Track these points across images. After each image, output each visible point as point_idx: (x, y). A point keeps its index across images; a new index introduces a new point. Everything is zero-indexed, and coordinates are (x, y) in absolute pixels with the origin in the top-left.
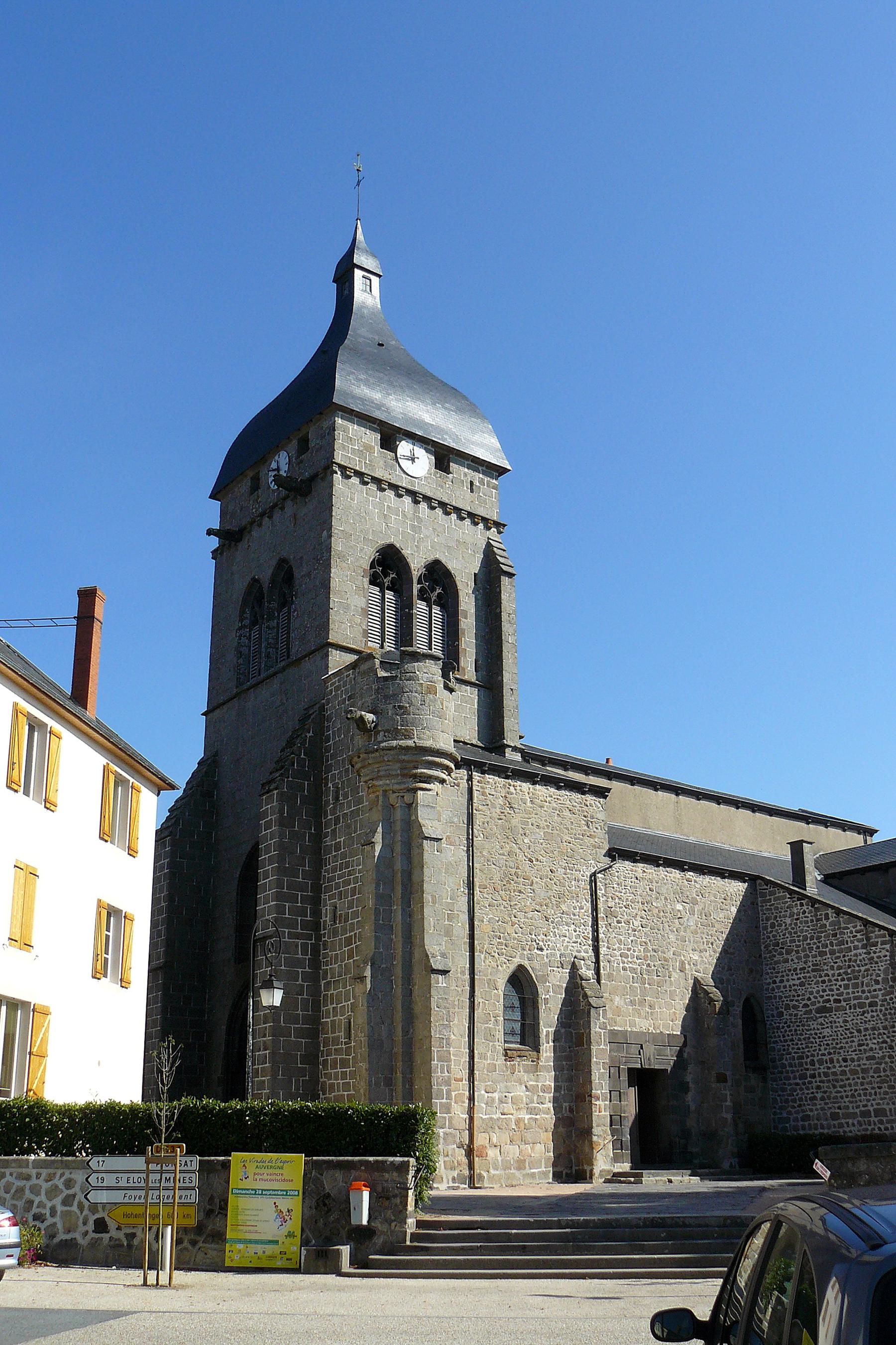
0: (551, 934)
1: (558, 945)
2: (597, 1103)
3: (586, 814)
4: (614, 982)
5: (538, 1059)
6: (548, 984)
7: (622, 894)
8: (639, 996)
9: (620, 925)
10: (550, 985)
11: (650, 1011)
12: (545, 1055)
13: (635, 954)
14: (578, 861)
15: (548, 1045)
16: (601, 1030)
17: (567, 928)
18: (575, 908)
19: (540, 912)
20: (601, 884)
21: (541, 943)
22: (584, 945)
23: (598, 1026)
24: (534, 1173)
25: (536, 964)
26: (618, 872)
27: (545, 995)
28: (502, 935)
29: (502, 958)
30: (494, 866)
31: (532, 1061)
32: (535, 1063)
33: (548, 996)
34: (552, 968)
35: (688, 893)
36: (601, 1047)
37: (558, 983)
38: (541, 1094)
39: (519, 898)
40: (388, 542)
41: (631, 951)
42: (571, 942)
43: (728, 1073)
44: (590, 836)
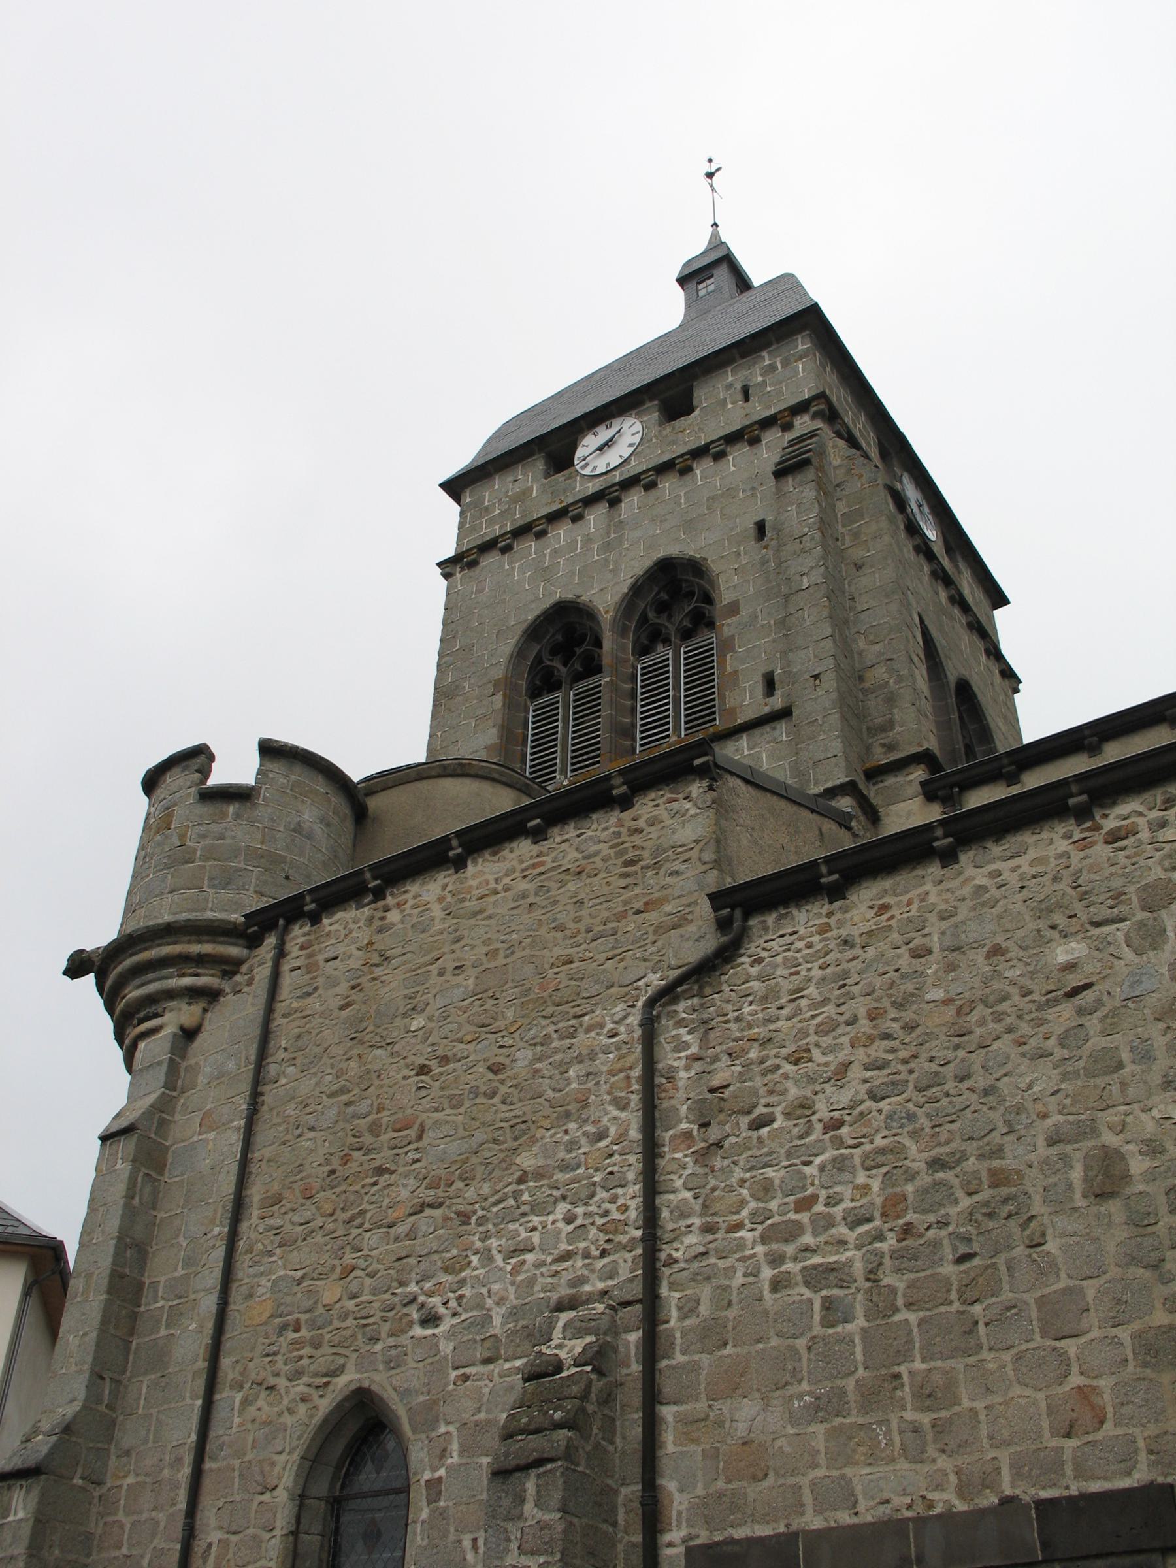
0: (475, 1259)
1: (495, 1287)
3: (631, 854)
4: (729, 1350)
6: (443, 1429)
7: (779, 1024)
8: (861, 1372)
10: (451, 1428)
11: (926, 1419)
13: (838, 1211)
17: (536, 1220)
18: (572, 1145)
19: (440, 1205)
20: (683, 1031)
21: (435, 1300)
22: (604, 1253)
23: (514, 1546)
25: (412, 1374)
26: (759, 961)
27: (434, 1469)
28: (303, 1317)
29: (300, 1388)
30: (311, 1134)
33: (442, 1472)
34: (462, 1371)
35: (1117, 883)
37: (482, 1416)
39: (376, 1188)
40: (547, 603)
41: (819, 1208)
42: (550, 1259)
44: (648, 906)
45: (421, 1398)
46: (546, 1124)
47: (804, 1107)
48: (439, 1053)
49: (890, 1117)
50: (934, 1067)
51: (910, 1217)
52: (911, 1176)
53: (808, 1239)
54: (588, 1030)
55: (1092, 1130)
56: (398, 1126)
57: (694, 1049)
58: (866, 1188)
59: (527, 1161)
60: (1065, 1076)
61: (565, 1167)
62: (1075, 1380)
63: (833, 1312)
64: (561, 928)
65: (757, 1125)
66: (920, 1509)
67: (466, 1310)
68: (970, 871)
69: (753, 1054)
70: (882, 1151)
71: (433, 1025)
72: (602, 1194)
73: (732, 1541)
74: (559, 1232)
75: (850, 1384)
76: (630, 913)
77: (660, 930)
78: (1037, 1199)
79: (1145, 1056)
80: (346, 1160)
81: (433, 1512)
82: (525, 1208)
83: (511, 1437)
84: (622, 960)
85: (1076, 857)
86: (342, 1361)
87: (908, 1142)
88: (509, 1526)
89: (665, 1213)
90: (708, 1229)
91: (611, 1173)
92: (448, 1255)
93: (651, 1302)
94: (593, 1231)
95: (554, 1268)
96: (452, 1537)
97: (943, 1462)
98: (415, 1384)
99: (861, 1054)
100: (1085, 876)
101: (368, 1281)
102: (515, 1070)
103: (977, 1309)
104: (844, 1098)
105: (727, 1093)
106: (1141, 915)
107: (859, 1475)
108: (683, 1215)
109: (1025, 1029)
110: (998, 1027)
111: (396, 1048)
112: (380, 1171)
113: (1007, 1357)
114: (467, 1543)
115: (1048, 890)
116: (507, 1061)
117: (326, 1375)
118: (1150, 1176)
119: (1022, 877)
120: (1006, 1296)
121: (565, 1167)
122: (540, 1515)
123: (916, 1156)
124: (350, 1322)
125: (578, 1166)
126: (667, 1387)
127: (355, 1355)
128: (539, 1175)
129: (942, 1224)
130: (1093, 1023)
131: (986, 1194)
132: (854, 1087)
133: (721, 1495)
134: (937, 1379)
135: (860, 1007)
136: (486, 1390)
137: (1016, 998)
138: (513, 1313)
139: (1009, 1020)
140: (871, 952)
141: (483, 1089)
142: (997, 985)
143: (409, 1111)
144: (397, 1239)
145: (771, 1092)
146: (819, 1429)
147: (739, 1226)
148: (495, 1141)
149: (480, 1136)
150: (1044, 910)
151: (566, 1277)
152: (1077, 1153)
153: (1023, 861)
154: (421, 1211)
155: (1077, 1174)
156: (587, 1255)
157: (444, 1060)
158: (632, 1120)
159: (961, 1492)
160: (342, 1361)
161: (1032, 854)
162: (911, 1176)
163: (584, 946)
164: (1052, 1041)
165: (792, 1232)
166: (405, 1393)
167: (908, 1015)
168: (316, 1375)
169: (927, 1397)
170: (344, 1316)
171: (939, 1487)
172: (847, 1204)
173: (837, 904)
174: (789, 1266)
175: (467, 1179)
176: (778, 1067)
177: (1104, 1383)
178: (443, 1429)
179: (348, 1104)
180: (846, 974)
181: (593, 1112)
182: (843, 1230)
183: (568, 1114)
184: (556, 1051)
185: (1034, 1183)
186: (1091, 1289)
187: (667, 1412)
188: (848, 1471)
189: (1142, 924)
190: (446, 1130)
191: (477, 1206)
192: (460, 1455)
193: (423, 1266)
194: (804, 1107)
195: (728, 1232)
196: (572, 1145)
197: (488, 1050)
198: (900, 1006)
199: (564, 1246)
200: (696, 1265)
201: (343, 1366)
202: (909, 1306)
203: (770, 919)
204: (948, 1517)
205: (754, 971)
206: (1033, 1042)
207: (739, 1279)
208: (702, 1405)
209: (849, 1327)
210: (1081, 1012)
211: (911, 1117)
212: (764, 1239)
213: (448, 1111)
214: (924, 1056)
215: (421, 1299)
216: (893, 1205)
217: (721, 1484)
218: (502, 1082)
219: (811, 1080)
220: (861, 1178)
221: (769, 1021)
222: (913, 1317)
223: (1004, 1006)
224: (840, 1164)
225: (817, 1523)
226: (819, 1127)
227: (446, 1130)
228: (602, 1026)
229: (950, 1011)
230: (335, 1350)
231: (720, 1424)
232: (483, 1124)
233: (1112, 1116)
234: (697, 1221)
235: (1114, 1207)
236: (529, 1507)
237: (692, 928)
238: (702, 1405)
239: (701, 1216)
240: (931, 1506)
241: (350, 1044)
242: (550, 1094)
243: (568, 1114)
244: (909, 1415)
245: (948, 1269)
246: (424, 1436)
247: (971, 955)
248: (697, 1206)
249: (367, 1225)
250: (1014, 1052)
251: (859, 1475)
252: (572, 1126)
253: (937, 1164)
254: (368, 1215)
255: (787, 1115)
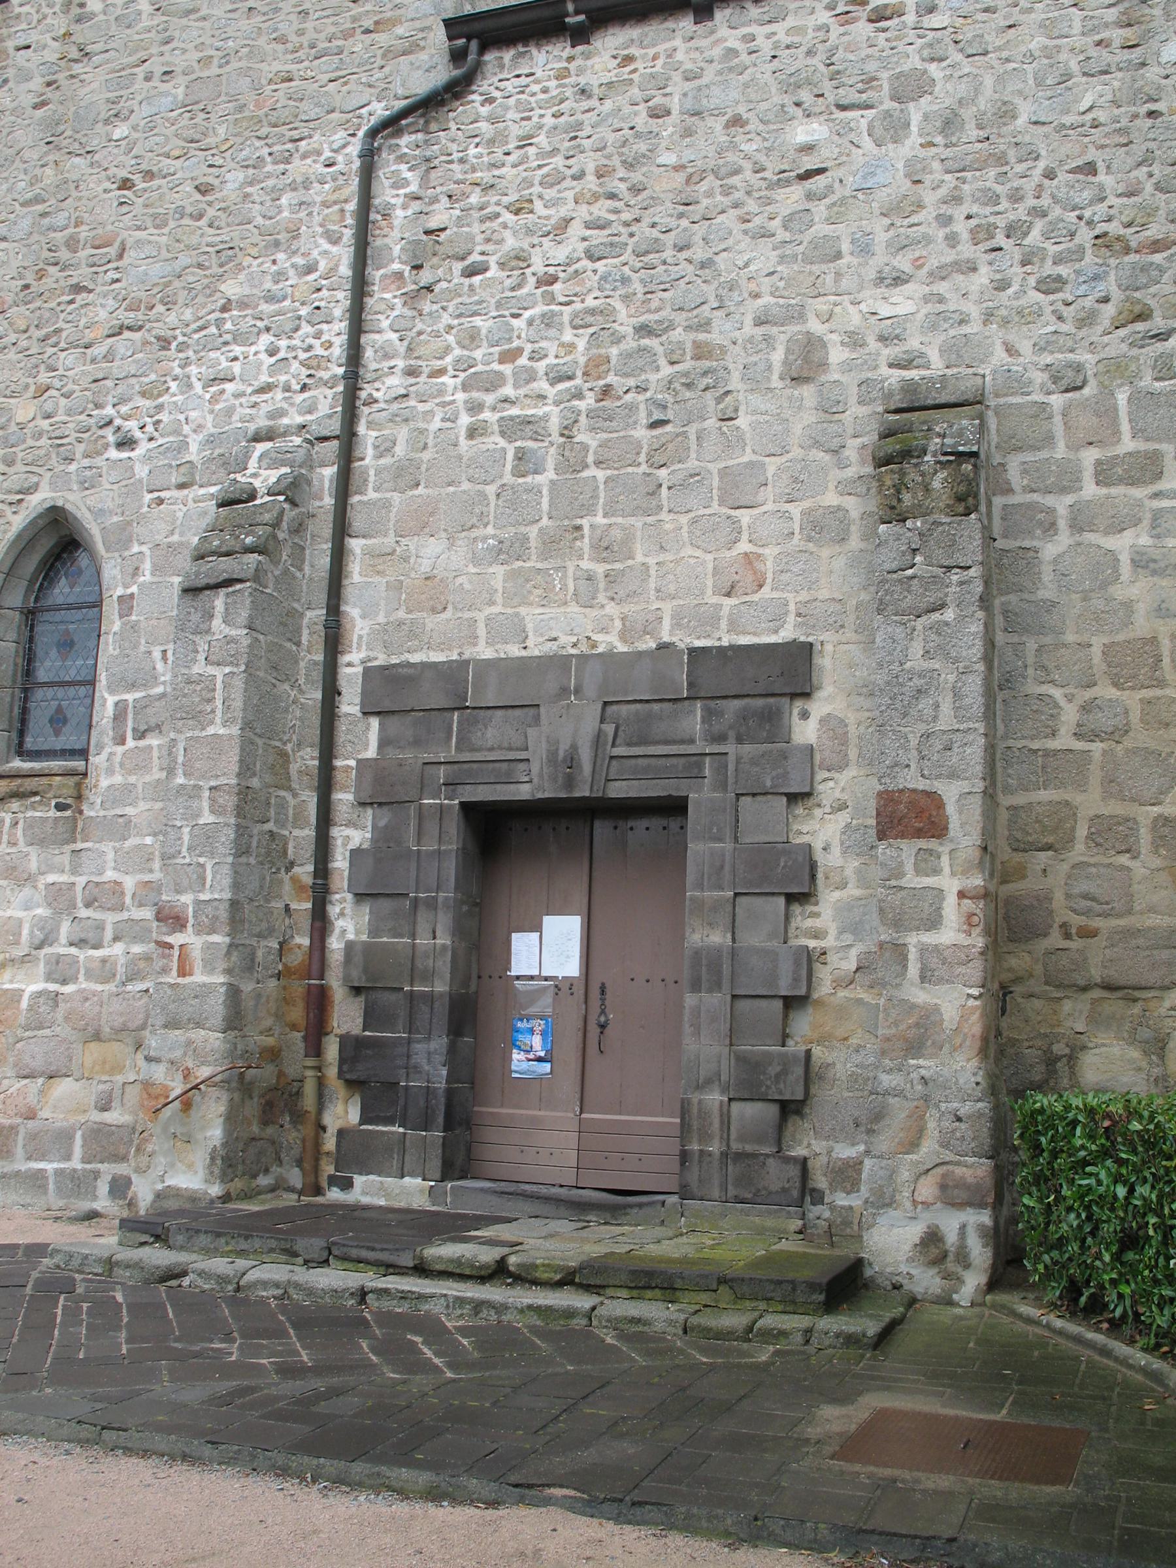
0: (173, 386)
1: (193, 415)
2: (176, 939)
4: (421, 490)
5: (79, 797)
6: (136, 549)
7: (503, 171)
8: (545, 521)
9: (477, 279)
10: (144, 548)
11: (600, 569)
12: (104, 783)
13: (541, 366)
14: (311, 125)
15: (120, 749)
16: (211, 670)
17: (238, 350)
18: (279, 277)
19: (140, 328)
20: (404, 167)
21: (132, 425)
22: (304, 388)
23: (201, 657)
24: (40, 1175)
25: (106, 496)
26: (490, 100)
27: (126, 587)
31: (60, 807)
32: (68, 813)
33: (134, 589)
34: (156, 494)
35: (871, 67)
36: (211, 730)
37: (175, 538)
38: (83, 913)
39: (73, 306)
41: (523, 361)
42: (249, 390)
43: (950, 792)
45: (115, 519)
46: (254, 252)
47: (520, 259)
48: (144, 167)
49: (604, 278)
50: (655, 233)
51: (611, 379)
52: (617, 339)
53: (508, 391)
54: (304, 157)
55: (800, 315)
56: (97, 243)
57: (413, 188)
58: (571, 347)
59: (231, 289)
60: (782, 259)
61: (270, 298)
62: (744, 546)
63: (525, 463)
64: (282, 40)
65: (470, 272)
66: (584, 648)
67: (162, 436)
68: (723, 31)
69: (474, 199)
70: (592, 312)
71: (135, 135)
72: (306, 329)
73: (409, 665)
74: (261, 363)
75: (533, 532)
76: (359, 31)
77: (389, 54)
78: (736, 376)
79: (864, 249)
80: (41, 275)
81: (124, 624)
82: (228, 337)
83: (202, 558)
84: (346, 83)
85: (836, 31)
86: (35, 479)
87: (618, 305)
88: (197, 639)
89: (369, 353)
90: (411, 372)
91: (318, 308)
92: (146, 380)
93: (348, 438)
94: (295, 365)
95: (254, 399)
96: (142, 649)
97: (611, 609)
98: (110, 504)
99: (583, 211)
100: (840, 54)
101: (63, 401)
102: (225, 192)
103: (663, 472)
104: (560, 254)
105: (443, 236)
106: (888, 105)
107: (531, 615)
108: (387, 357)
109: (752, 206)
110: (726, 201)
111: (97, 157)
112: (78, 289)
113: (684, 520)
114: (157, 655)
115: (798, 64)
116: (216, 182)
117: (19, 492)
118: (847, 367)
119: (776, 46)
120: (692, 464)
121: (270, 298)
122: (227, 630)
123: (625, 320)
124: (44, 441)
125: (284, 298)
126: (358, 520)
127: (50, 474)
128: (243, 305)
129: (641, 389)
130: (820, 210)
131: (687, 365)
132: (573, 244)
133: (401, 623)
134: (616, 533)
135: (589, 162)
136: (180, 514)
137: (748, 174)
138: (210, 441)
139: (737, 195)
140: (608, 105)
141: (189, 210)
142: (731, 157)
143: (110, 227)
144: (93, 361)
145: (488, 240)
146: (499, 570)
147: (442, 372)
148: (200, 266)
149: (184, 260)
150: (791, 85)
151: (265, 408)
152: (782, 336)
153: (779, 28)
154: (120, 334)
155: (778, 356)
156: (287, 389)
157: (149, 175)
158: (344, 255)
159: (623, 637)
160: (35, 479)
161: (790, 22)
162: (617, 339)
163: (306, 63)
164: (777, 222)
165: (493, 382)
166: (99, 513)
167: (637, 177)
168: (9, 492)
169: (604, 549)
170: (39, 435)
171: (604, 630)
172: (551, 360)
173: (580, 48)
174: (486, 415)
175: (169, 303)
176: (497, 215)
177: (769, 552)
178: (136, 549)
179: (44, 215)
180: (579, 125)
181: (303, 243)
182: (542, 385)
183: (277, 244)
184: (269, 176)
185: (735, 360)
186: (772, 466)
187: (355, 545)
188: (523, 610)
189: (888, 114)
190: (148, 250)
191: (178, 332)
192: (153, 574)
193: (120, 390)
194: (520, 259)
195: (429, 377)
196: (279, 277)
197: (195, 168)
198: (629, 166)
199: (264, 378)
200: (395, 406)
201: (37, 484)
202: (598, 463)
203: (508, 55)
204: (609, 657)
205: (484, 111)
206: (757, 221)
207: (436, 423)
208: (390, 539)
209: (539, 478)
210: (810, 196)
211: (625, 280)
212: (465, 387)
213: (152, 231)
214: (646, 221)
215: (118, 422)
216: (596, 366)
217: (401, 614)
218: (210, 204)
219: (529, 232)
220: (568, 336)
221: (494, 166)
222: (601, 475)
223: (735, 180)
224: (548, 320)
225: (487, 654)
226: (532, 281)
227: (148, 250)
228: (319, 153)
229: (680, 177)
230: (29, 468)
231: (406, 559)
232: (188, 247)
233: (821, 305)
234: (400, 363)
235: (807, 392)
236: (217, 623)
237: (423, 56)
238: (390, 539)
239: (405, 358)
240: (594, 646)
241: (46, 148)
242: (259, 221)
243: (277, 244)
244: (585, 564)
245: (641, 433)
246: (116, 554)
247: (710, 122)
248: (402, 348)
249: (63, 345)
250: (737, 228)
251: (531, 615)
252: (281, 256)
253: (644, 330)
254: (64, 334)
255: (502, 265)
